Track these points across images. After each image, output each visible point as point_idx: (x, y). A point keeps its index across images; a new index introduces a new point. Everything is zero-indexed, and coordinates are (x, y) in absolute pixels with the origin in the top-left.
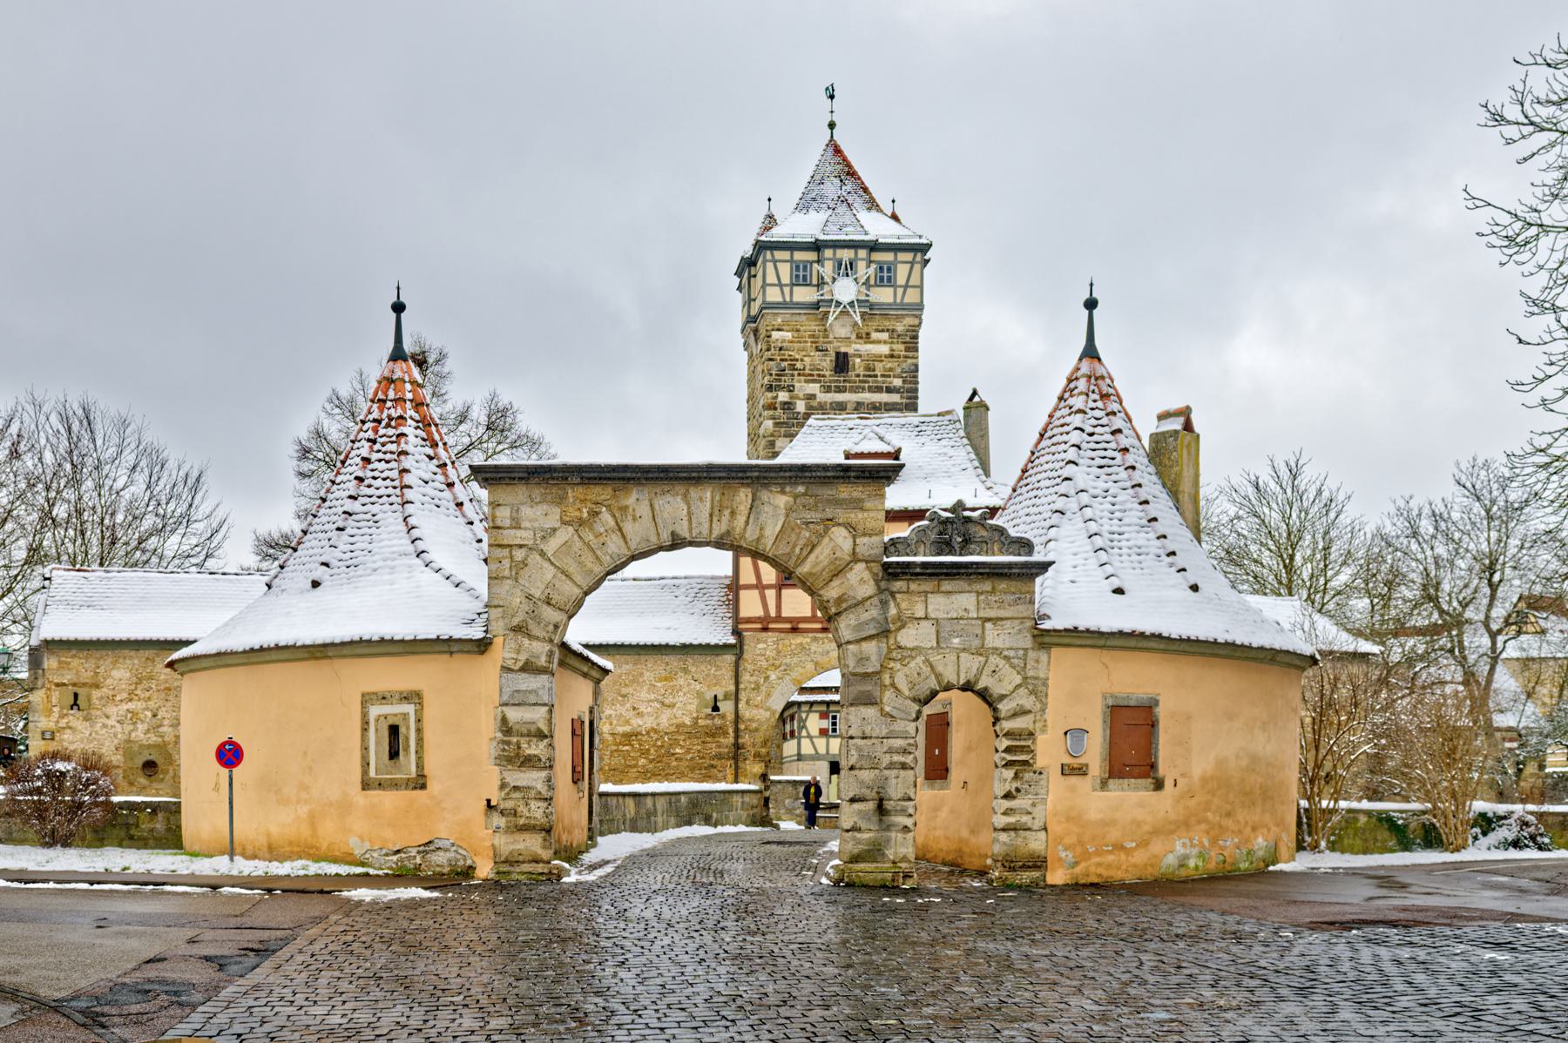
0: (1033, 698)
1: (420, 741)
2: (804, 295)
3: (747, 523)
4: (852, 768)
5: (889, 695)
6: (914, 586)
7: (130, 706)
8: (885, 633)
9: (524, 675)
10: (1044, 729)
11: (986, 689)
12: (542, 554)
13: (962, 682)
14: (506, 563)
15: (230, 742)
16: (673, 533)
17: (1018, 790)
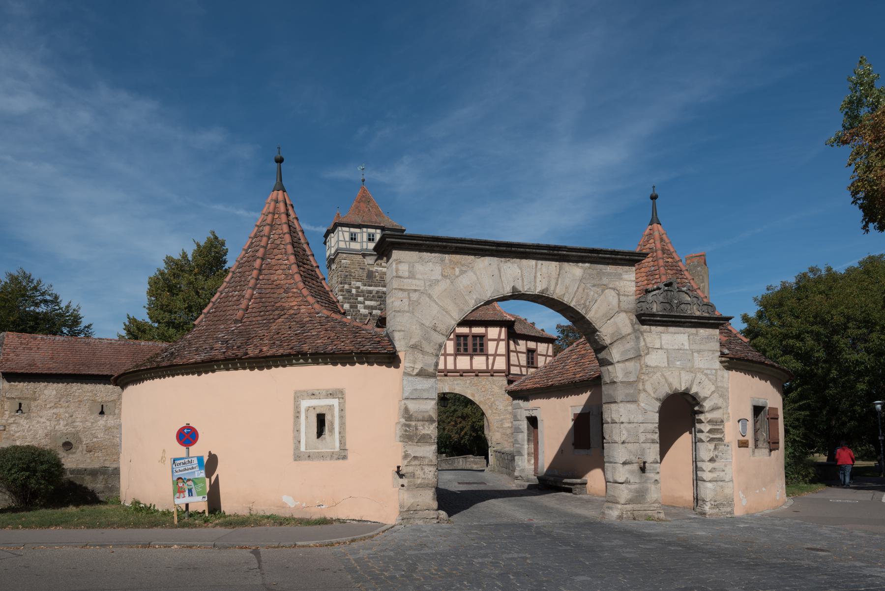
0: (721, 399)
1: (342, 425)
2: (355, 246)
3: (557, 284)
4: (623, 443)
5: (642, 396)
6: (653, 328)
7: (55, 411)
8: (638, 357)
9: (419, 379)
10: (728, 420)
11: (697, 393)
12: (430, 296)
13: (683, 389)
14: (406, 301)
15: (188, 427)
16: (514, 288)
17: (717, 456)
